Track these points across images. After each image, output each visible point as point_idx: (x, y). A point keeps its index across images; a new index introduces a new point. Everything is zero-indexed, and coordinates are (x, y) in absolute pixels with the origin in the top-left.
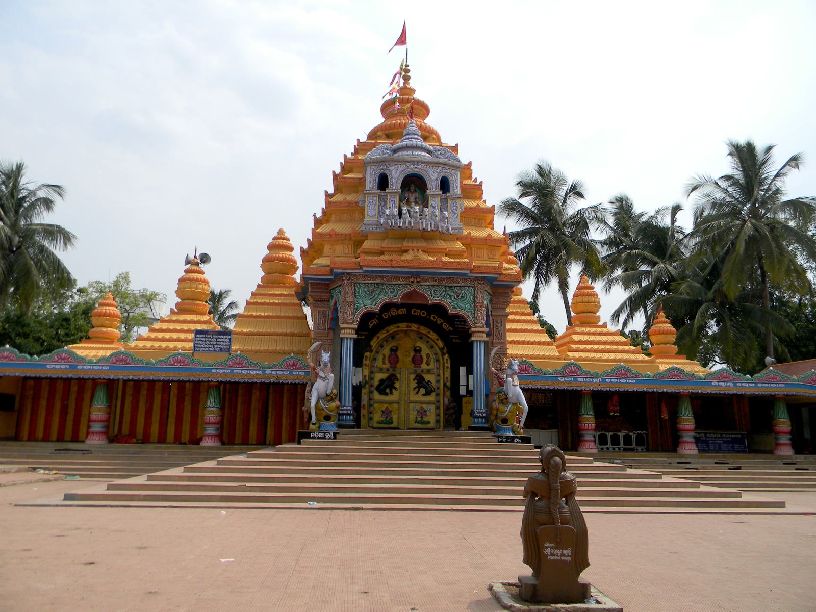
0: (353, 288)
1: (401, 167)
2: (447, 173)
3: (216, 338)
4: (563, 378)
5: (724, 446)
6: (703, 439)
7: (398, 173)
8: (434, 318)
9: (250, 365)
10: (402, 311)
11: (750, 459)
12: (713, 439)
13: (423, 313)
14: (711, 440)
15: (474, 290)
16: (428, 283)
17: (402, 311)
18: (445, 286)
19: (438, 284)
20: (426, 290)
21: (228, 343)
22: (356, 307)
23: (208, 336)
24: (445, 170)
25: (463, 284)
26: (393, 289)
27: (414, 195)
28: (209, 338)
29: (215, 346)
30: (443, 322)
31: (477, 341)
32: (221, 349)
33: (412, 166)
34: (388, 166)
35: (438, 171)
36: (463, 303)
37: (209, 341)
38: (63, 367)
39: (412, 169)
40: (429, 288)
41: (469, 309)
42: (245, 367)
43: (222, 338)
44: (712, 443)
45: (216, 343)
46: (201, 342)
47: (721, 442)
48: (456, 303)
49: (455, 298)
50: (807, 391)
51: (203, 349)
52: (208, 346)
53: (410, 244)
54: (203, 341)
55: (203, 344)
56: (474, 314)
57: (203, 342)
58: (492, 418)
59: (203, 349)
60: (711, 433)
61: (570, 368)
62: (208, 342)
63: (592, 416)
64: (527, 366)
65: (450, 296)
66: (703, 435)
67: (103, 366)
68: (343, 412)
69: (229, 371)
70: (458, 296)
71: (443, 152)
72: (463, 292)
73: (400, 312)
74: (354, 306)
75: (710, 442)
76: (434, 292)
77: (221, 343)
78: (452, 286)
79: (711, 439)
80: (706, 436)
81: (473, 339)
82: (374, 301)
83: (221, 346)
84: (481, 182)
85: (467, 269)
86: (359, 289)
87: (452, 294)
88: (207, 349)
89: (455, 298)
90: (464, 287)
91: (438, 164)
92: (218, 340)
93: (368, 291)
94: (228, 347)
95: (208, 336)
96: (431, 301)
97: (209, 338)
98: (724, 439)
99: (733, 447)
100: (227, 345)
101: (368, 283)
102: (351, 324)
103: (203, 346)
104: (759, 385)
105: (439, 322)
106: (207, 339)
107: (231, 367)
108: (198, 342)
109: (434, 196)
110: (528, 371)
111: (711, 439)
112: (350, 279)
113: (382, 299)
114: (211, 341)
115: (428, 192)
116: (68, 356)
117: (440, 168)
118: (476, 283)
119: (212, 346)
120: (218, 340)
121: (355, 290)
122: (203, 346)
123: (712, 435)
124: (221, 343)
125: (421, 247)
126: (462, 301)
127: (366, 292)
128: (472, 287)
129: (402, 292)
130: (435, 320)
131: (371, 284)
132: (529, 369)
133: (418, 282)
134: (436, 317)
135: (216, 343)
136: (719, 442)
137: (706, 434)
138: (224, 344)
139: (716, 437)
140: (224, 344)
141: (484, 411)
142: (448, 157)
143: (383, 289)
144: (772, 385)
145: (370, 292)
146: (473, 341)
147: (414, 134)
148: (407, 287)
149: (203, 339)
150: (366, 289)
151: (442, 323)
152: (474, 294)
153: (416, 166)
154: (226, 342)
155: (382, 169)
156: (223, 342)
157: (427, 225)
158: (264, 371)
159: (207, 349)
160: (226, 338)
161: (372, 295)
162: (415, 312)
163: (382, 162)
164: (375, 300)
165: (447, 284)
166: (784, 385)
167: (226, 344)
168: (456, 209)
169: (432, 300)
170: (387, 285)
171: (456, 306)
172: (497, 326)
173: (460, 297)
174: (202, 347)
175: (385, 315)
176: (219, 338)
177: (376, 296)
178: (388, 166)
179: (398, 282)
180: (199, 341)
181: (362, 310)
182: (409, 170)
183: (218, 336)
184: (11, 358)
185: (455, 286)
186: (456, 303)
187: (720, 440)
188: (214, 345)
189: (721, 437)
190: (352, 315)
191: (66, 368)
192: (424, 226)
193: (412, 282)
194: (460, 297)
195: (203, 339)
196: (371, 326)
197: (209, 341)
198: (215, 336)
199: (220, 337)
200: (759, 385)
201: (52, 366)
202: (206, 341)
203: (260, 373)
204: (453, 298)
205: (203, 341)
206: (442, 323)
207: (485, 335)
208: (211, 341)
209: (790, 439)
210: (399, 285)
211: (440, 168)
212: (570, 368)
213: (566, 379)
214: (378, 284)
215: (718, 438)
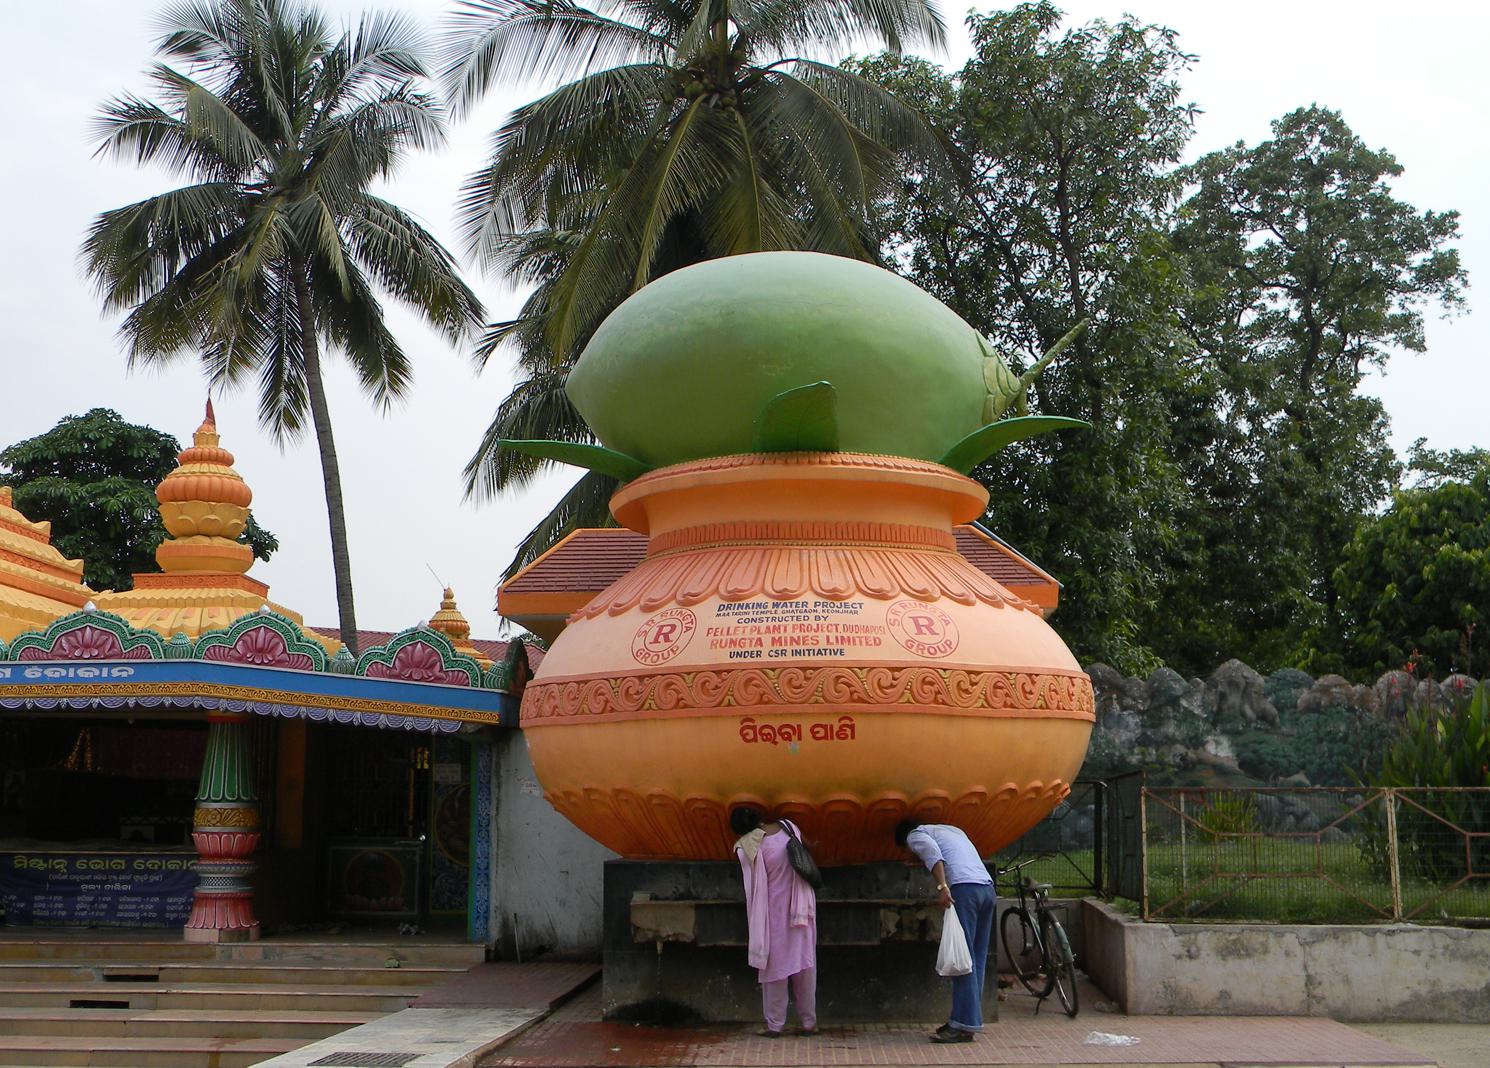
5: (129, 907)
6: (58, 877)
11: (40, 956)
12: (96, 878)
14: (87, 882)
44: (89, 892)
47: (125, 887)
50: (260, 693)
60: (89, 857)
66: (61, 865)
75: (84, 887)
79: (89, 877)
80: (72, 870)
98: (137, 878)
99: (161, 910)
104: (28, 673)
111: (89, 877)
123: (97, 864)
136: (117, 887)
137: (71, 859)
139: (111, 871)
144: (81, 672)
166: (131, 671)
187: (123, 883)
189: (129, 869)
200: (28, 673)
209: (239, 880)
215: (119, 873)
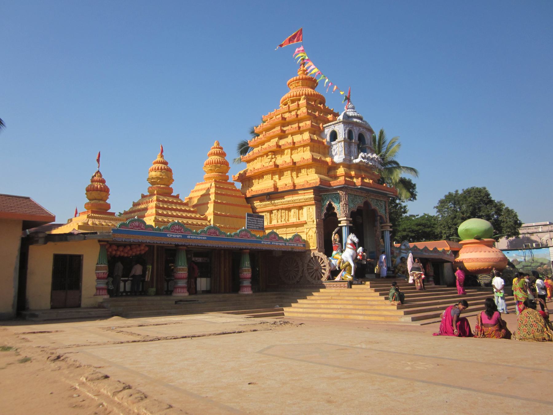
3: (257, 220)
21: (262, 224)
31: (386, 231)
37: (253, 222)
38: (178, 236)
42: (277, 240)
43: (260, 220)
45: (256, 223)
51: (251, 227)
52: (253, 225)
55: (250, 223)
58: (397, 270)
59: (251, 227)
62: (253, 223)
63: (249, 268)
67: (203, 237)
77: (259, 223)
83: (259, 226)
88: (253, 227)
92: (258, 221)
94: (262, 226)
106: (253, 220)
114: (254, 222)
116: (181, 228)
119: (255, 225)
120: (258, 221)
124: (259, 223)
138: (260, 224)
140: (260, 224)
149: (251, 220)
156: (260, 223)
158: (285, 243)
159: (253, 227)
176: (258, 220)
184: (142, 227)
191: (180, 237)
195: (251, 220)
197: (253, 222)
198: (256, 219)
199: (259, 219)
201: (171, 235)
202: (252, 221)
203: (284, 244)
207: (389, 227)
209: (433, 279)
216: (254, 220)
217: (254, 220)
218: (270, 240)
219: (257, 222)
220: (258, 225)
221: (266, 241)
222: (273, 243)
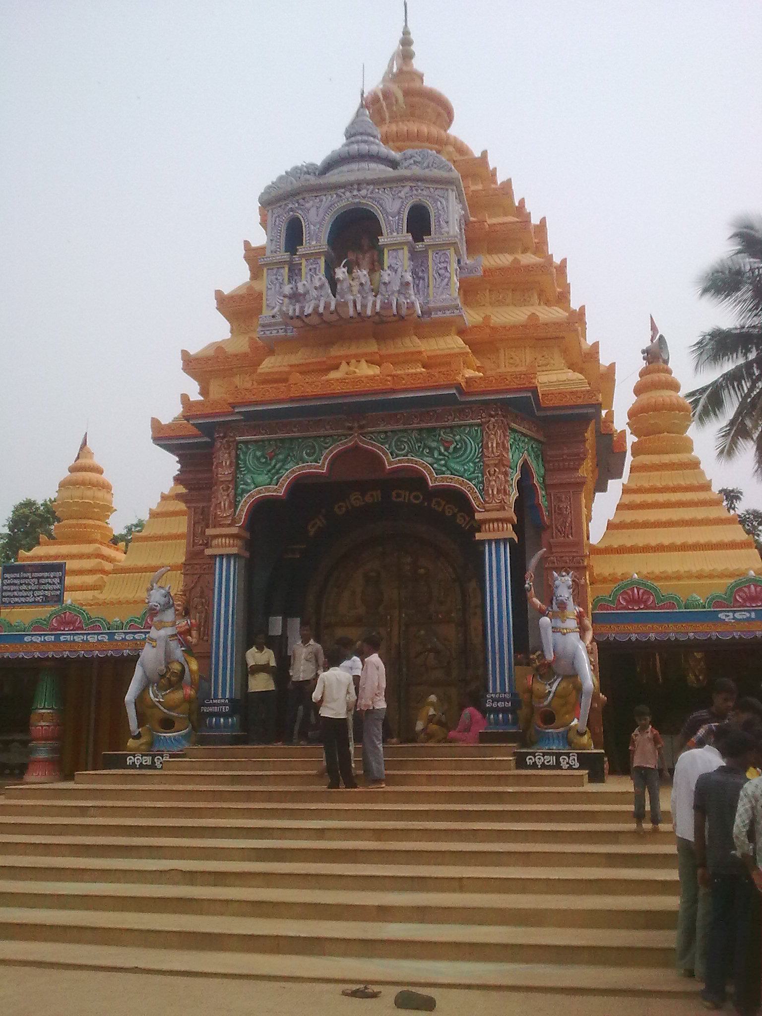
0: (233, 452)
1: (327, 199)
2: (422, 196)
3: (38, 578)
4: (731, 614)
7: (321, 210)
8: (438, 504)
9: (87, 625)
10: (372, 496)
13: (416, 498)
15: (482, 431)
16: (381, 428)
17: (372, 496)
18: (420, 430)
19: (401, 427)
20: (378, 442)
21: (58, 587)
22: (239, 491)
23: (25, 575)
24: (417, 190)
25: (457, 422)
26: (314, 447)
27: (368, 255)
28: (26, 578)
29: (37, 593)
30: (459, 512)
31: (490, 541)
32: (46, 597)
33: (348, 194)
34: (301, 201)
35: (402, 194)
36: (457, 463)
37: (25, 584)
39: (347, 200)
40: (387, 436)
41: (473, 472)
43: (48, 578)
45: (36, 587)
46: (13, 588)
48: (443, 462)
49: (441, 454)
51: (17, 600)
53: (342, 352)
54: (16, 584)
56: (482, 482)
57: (16, 588)
59: (17, 600)
61: (746, 590)
62: (24, 587)
64: (641, 591)
65: (430, 448)
68: (211, 709)
69: (53, 637)
70: (447, 449)
71: (419, 159)
72: (458, 437)
73: (368, 499)
74: (236, 488)
76: (396, 445)
78: (434, 429)
81: (478, 536)
82: (274, 475)
84: (543, 221)
85: (448, 387)
86: (245, 454)
87: (434, 445)
88: (23, 600)
89: (441, 454)
90: (460, 426)
91: (402, 180)
93: (263, 456)
94: (58, 593)
95: (25, 575)
96: (390, 463)
97: (26, 578)
100: (57, 590)
101: (263, 441)
102: (229, 525)
103: (16, 593)
105: (448, 513)
106: (22, 581)
107: (56, 630)
108: (8, 588)
109: (396, 247)
110: (645, 602)
112: (224, 437)
113: (292, 471)
114: (29, 584)
115: (382, 240)
117: (407, 189)
118: (484, 415)
121: (237, 457)
122: (16, 593)
125: (365, 354)
126: (457, 458)
127: (258, 459)
128: (479, 425)
129: (331, 451)
130: (440, 510)
131: (269, 440)
132: (649, 598)
133: (362, 427)
134: (443, 503)
135: (36, 587)
138: (50, 587)
140: (50, 587)
141: (508, 696)
142: (428, 167)
143: (292, 449)
145: (266, 458)
146: (482, 542)
147: (361, 134)
148: (341, 440)
150: (259, 454)
151: (454, 515)
152: (482, 441)
153: (355, 193)
154: (54, 584)
155: (292, 210)
157: (364, 306)
158: (111, 635)
159: (23, 600)
160: (54, 577)
161: (270, 464)
162: (398, 496)
163: (288, 197)
164: (277, 472)
165: (424, 425)
167: (55, 587)
168: (446, 268)
169: (391, 462)
170: (300, 440)
171: (444, 469)
172: (560, 509)
173: (451, 450)
174: (14, 596)
175: (340, 507)
176: (43, 577)
177: (278, 466)
178: (301, 201)
179: (322, 432)
180: (8, 584)
181: (252, 496)
182: (343, 203)
183: (41, 574)
185: (442, 428)
186: (443, 462)
188: (34, 591)
190: (230, 507)
192: (359, 308)
193: (350, 428)
194: (451, 450)
196: (312, 532)
197: (25, 584)
198: (36, 575)
199: (46, 574)
202: (21, 584)
204: (436, 454)
205: (16, 584)
206: (454, 515)
208: (29, 584)
210: (325, 437)
211: (407, 189)
212: (746, 590)
213: (737, 615)
214: (282, 440)
216: (27, 581)
217: (27, 581)
218: (52, 630)
219: (39, 584)
220: (41, 593)
221: (40, 635)
222: (62, 638)
